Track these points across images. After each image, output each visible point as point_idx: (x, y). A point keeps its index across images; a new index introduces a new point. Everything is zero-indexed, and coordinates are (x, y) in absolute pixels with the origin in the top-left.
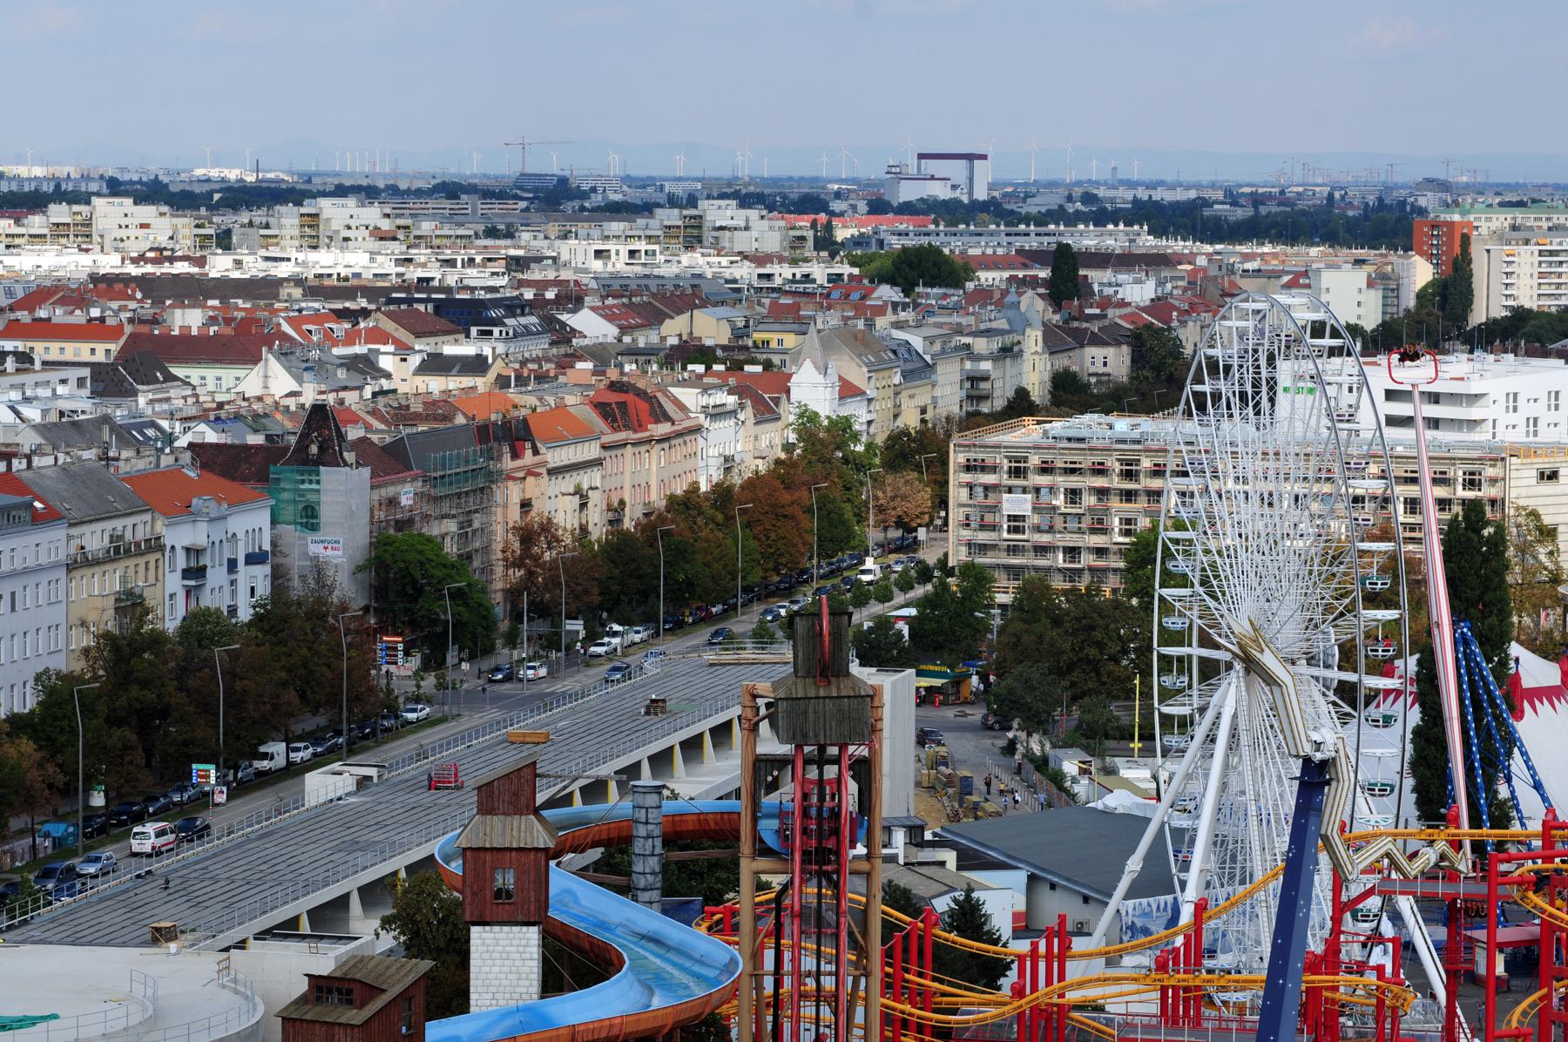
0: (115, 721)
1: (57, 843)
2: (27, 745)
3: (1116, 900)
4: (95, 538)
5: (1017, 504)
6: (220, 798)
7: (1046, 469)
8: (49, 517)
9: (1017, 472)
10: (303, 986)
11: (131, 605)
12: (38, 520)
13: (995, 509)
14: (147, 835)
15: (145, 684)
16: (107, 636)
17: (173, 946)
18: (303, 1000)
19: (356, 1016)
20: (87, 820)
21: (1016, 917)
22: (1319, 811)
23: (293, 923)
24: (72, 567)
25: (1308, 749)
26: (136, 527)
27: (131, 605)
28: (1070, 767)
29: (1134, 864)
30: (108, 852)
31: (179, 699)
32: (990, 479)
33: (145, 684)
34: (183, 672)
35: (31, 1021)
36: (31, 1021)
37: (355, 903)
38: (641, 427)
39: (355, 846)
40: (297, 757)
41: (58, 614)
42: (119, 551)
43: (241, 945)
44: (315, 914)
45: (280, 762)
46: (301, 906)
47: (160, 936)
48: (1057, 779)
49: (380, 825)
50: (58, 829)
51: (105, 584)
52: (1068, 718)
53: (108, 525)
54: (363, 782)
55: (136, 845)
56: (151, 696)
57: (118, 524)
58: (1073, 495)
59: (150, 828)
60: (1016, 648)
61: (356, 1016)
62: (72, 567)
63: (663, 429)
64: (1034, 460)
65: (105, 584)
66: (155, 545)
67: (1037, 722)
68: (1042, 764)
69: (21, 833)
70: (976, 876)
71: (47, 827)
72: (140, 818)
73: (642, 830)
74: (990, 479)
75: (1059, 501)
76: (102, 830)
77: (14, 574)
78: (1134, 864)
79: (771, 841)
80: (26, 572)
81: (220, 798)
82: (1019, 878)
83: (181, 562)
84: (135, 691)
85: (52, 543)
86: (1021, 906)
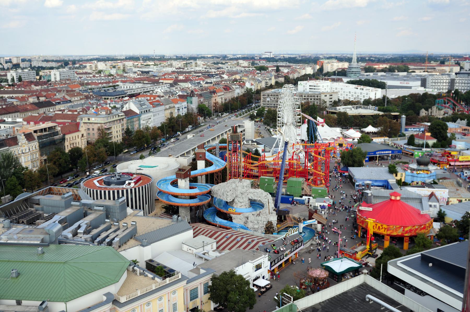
0: (169, 128)
1: (163, 141)
2: (160, 131)
3: (273, 148)
4: (167, 107)
5: (268, 99)
6: (181, 135)
7: (271, 95)
8: (162, 105)
9: (268, 96)
10: (178, 169)
11: (171, 113)
12: (161, 105)
13: (266, 100)
14: (172, 140)
15: (172, 123)
16: (168, 118)
17: (171, 157)
18: (178, 171)
19: (183, 173)
20: (166, 138)
21: (262, 150)
22: (287, 147)
23: (184, 154)
24: (165, 110)
25: (286, 141)
26: (172, 105)
27: (171, 113)
28: (272, 130)
29: (274, 145)
30: (168, 142)
31: (176, 125)
32: (265, 97)
33: (172, 123)
34: (177, 121)
35: (156, 167)
36: (156, 167)
37: (191, 151)
38: (228, 90)
39: (192, 144)
40: (189, 130)
41: (164, 115)
42: (170, 108)
43: (178, 157)
44: (187, 153)
45: (187, 131)
46: (185, 152)
47: (170, 156)
48: (270, 132)
49: (195, 141)
50: (163, 139)
51: (169, 111)
52: (272, 125)
53: (169, 105)
54: (193, 136)
55: (171, 141)
56: (173, 125)
57: (170, 105)
58: (274, 98)
59: (173, 139)
60: (267, 117)
61: (183, 173)
62: (165, 110)
63: (231, 90)
64: (270, 94)
65: (169, 111)
66: (174, 107)
67: (268, 125)
68: (269, 130)
69: (159, 140)
70: (258, 146)
71: (162, 139)
72: (172, 138)
73: (217, 148)
74: (265, 97)
75: (273, 99)
76: (168, 139)
77: (159, 111)
78: (274, 145)
79: (230, 150)
80: (160, 111)
81: (181, 135)
82: (263, 146)
83: (177, 109)
84: (171, 124)
85: (163, 108)
86: (263, 149)
